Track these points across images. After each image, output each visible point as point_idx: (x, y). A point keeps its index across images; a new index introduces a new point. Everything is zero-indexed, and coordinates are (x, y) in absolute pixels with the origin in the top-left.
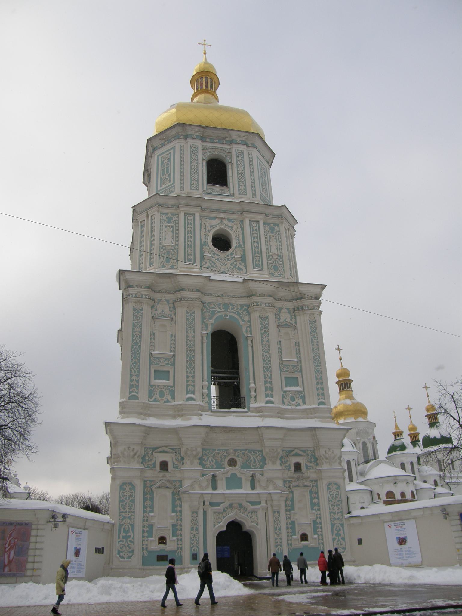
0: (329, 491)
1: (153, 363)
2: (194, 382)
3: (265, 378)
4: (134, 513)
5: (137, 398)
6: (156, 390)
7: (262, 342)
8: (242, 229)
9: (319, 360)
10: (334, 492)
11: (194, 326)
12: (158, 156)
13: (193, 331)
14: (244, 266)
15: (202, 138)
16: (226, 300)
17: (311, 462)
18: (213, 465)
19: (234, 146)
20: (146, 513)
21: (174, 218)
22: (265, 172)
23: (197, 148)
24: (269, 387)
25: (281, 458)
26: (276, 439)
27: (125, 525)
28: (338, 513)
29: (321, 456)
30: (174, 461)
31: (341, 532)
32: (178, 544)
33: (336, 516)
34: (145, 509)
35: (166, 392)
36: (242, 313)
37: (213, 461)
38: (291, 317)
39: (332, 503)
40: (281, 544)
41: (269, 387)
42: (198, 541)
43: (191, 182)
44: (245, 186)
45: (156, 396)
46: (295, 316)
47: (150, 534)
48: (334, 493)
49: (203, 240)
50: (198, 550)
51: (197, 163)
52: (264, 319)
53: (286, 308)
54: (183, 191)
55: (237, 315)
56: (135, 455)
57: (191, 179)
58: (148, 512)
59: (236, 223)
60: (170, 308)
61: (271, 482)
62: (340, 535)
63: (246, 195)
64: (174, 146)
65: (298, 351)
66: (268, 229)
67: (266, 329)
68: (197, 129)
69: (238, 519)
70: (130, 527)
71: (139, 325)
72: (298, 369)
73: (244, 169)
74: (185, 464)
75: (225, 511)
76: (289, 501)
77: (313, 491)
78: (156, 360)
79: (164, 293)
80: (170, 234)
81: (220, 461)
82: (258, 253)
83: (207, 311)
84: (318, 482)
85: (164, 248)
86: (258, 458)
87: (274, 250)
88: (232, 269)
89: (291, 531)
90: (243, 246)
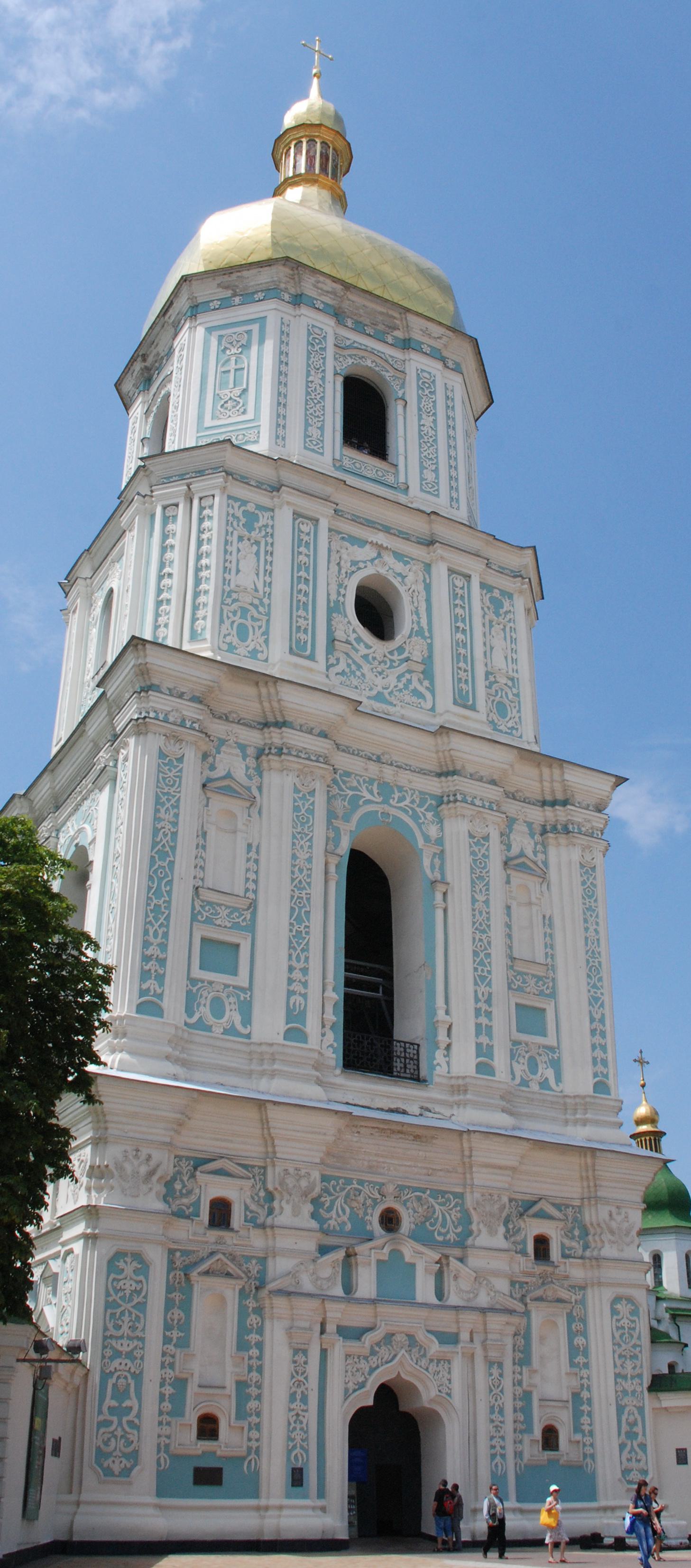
0: (615, 1317)
1: (199, 917)
2: (305, 984)
3: (477, 1000)
4: (143, 1343)
5: (158, 1011)
6: (205, 994)
7: (473, 904)
8: (428, 588)
9: (598, 973)
10: (625, 1322)
11: (312, 831)
13: (308, 844)
14: (427, 688)
15: (338, 315)
16: (388, 773)
17: (573, 1238)
18: (344, 1223)
19: (413, 355)
20: (170, 1344)
24: (484, 1026)
25: (506, 1222)
26: (500, 1167)
27: (119, 1377)
28: (633, 1377)
29: (599, 1225)
30: (248, 1201)
31: (638, 1429)
32: (249, 1439)
33: (628, 1385)
34: (168, 1334)
35: (230, 1003)
36: (424, 815)
37: (343, 1210)
38: (535, 848)
39: (619, 1351)
40: (503, 1452)
41: (484, 1026)
42: (306, 1432)
43: (306, 430)
44: (436, 471)
45: (204, 1011)
46: (545, 845)
48: (626, 1326)
49: (333, 597)
50: (305, 1456)
51: (323, 378)
52: (479, 841)
53: (525, 822)
54: (284, 446)
55: (410, 816)
56: (151, 1173)
57: (306, 420)
58: (175, 1340)
59: (414, 568)
60: (247, 768)
61: (485, 1282)
62: (636, 1435)
63: (437, 496)
64: (262, 315)
65: (548, 938)
66: (487, 599)
67: (484, 868)
68: (329, 285)
69: (403, 1376)
70: (130, 1380)
71: (173, 801)
72: (548, 988)
73: (436, 426)
74: (277, 1211)
75: (373, 1353)
76: (519, 1337)
77: (575, 1314)
78: (207, 908)
79: (232, 722)
80: (252, 558)
81: (361, 1213)
82: (465, 662)
83: (341, 795)
84: (589, 1291)
85: (234, 596)
86: (453, 1213)
87: (499, 661)
88: (400, 690)
89: (522, 1419)
90: (427, 634)
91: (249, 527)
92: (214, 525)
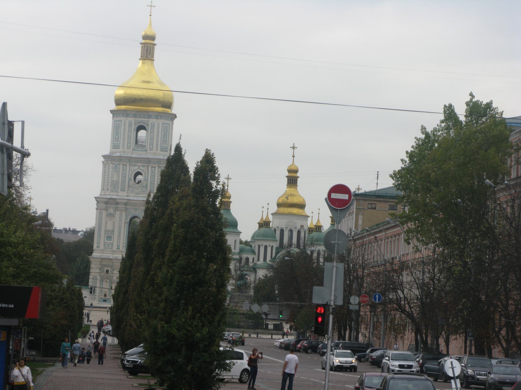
2: (120, 242)
8: (148, 171)
12: (115, 121)
15: (135, 116)
16: (136, 207)
19: (150, 120)
21: (118, 166)
22: (167, 130)
23: (132, 123)
44: (153, 145)
45: (106, 246)
47: (101, 294)
49: (130, 177)
51: (131, 132)
91: (116, 169)
92: (111, 170)
